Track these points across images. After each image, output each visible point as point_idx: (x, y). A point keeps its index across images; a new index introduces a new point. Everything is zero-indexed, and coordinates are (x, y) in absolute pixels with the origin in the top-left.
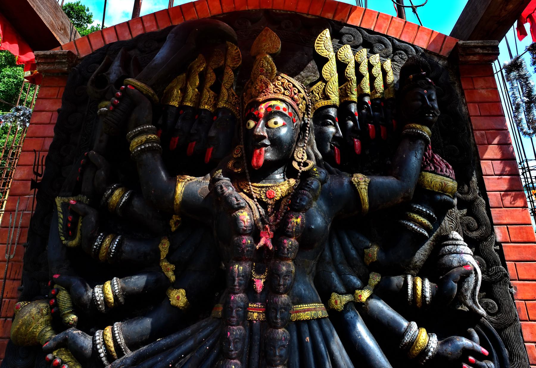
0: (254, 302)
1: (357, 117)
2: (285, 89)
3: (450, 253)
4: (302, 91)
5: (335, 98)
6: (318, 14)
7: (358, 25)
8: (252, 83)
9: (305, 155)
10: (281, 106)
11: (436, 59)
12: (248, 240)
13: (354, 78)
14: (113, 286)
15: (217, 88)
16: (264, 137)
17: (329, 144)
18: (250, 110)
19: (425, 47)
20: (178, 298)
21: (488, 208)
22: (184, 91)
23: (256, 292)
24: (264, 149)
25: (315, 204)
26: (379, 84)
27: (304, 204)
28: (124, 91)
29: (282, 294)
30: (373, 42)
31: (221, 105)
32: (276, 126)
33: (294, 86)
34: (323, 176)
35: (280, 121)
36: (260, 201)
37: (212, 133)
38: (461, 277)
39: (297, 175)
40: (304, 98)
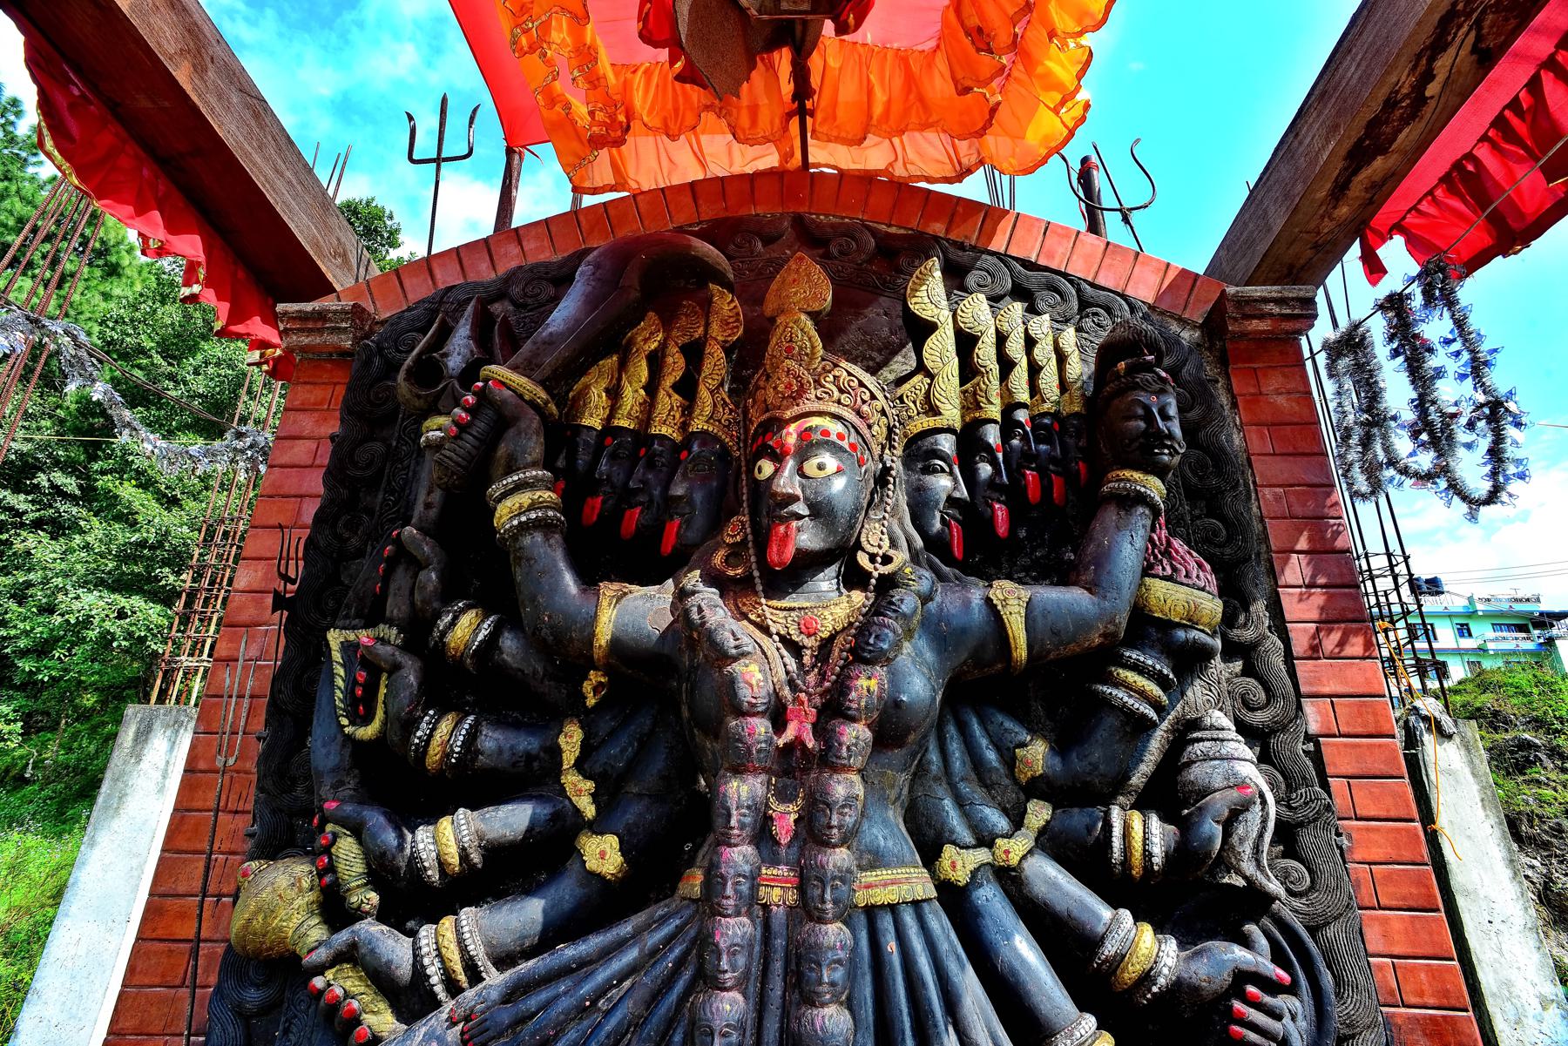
0: (775, 862)
1: (1000, 455)
2: (841, 391)
3: (1207, 758)
4: (879, 395)
5: (952, 414)
6: (914, 225)
7: (1002, 250)
8: (768, 377)
9: (885, 537)
11: (1175, 327)
12: (761, 726)
13: (995, 368)
14: (456, 828)
15: (687, 388)
16: (793, 499)
17: (938, 515)
18: (764, 441)
19: (1151, 301)
20: (603, 855)
21: (1289, 657)
22: (614, 394)
23: (778, 843)
24: (794, 524)
25: (907, 647)
26: (1049, 380)
27: (885, 646)
28: (482, 395)
29: (835, 846)
30: (1033, 287)
31: (698, 424)
32: (822, 474)
33: (861, 384)
34: (924, 585)
35: (831, 463)
36: (786, 641)
37: (679, 490)
38: (1231, 811)
39: (869, 584)
40: (883, 412)
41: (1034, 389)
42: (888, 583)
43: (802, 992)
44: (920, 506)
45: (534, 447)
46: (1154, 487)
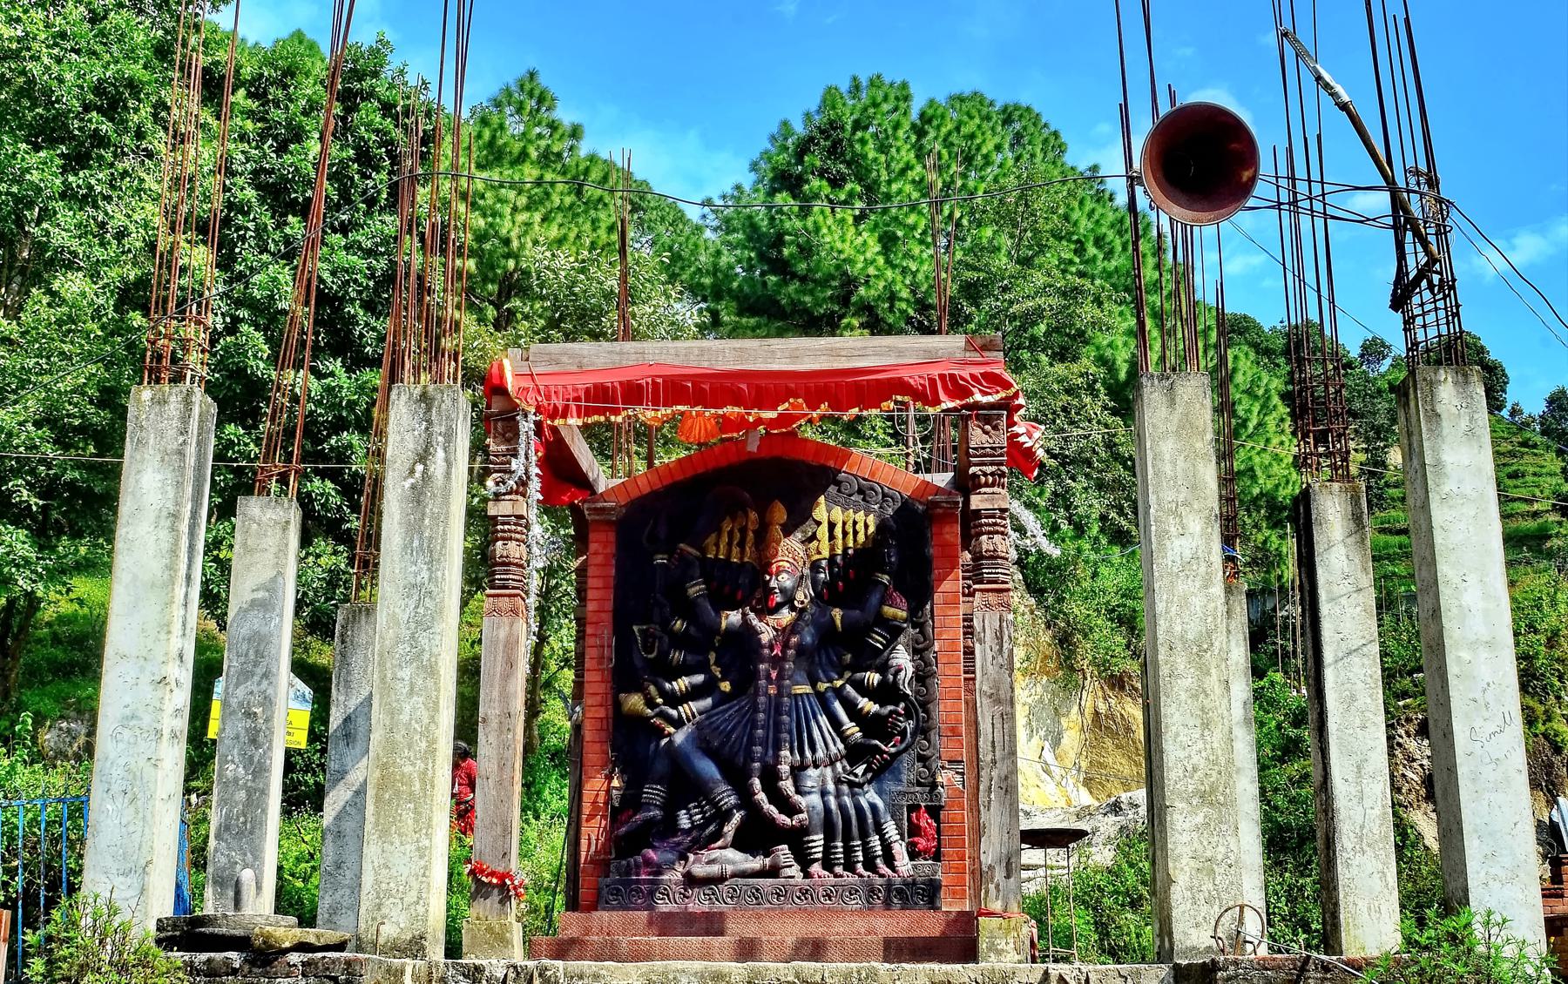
5: (826, 554)
10: (790, 562)
12: (766, 651)
15: (742, 544)
22: (717, 545)
35: (784, 575)
41: (855, 540)
42: (803, 610)
43: (779, 712)
44: (815, 582)
45: (697, 572)
46: (885, 579)
